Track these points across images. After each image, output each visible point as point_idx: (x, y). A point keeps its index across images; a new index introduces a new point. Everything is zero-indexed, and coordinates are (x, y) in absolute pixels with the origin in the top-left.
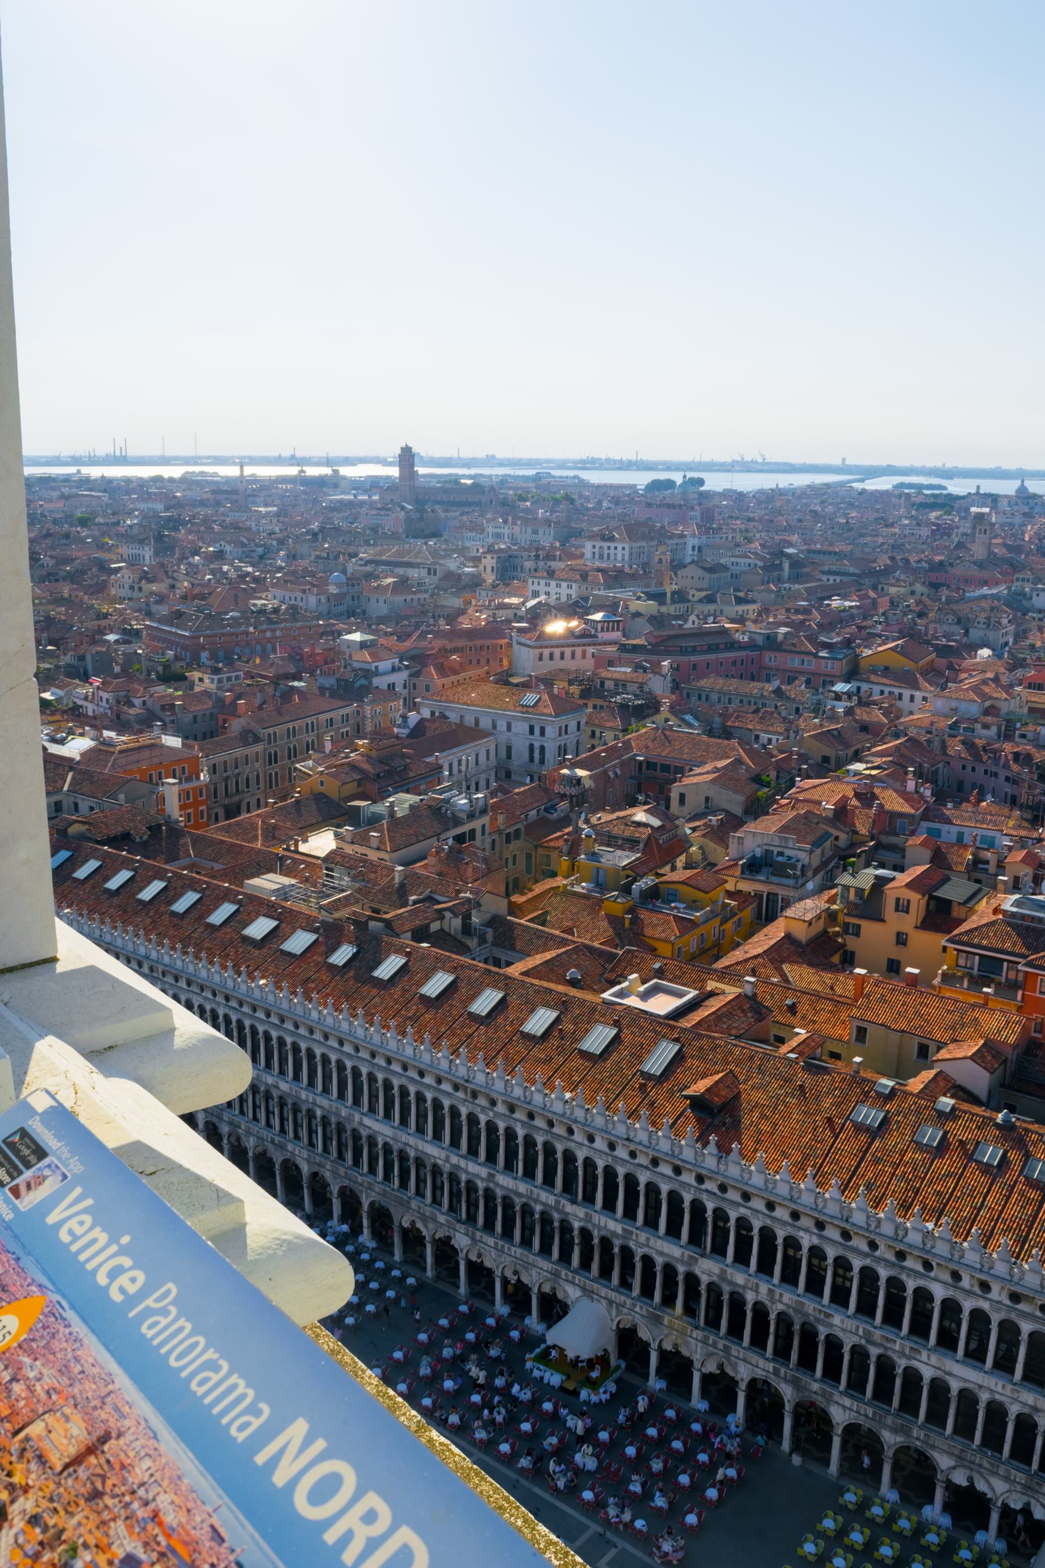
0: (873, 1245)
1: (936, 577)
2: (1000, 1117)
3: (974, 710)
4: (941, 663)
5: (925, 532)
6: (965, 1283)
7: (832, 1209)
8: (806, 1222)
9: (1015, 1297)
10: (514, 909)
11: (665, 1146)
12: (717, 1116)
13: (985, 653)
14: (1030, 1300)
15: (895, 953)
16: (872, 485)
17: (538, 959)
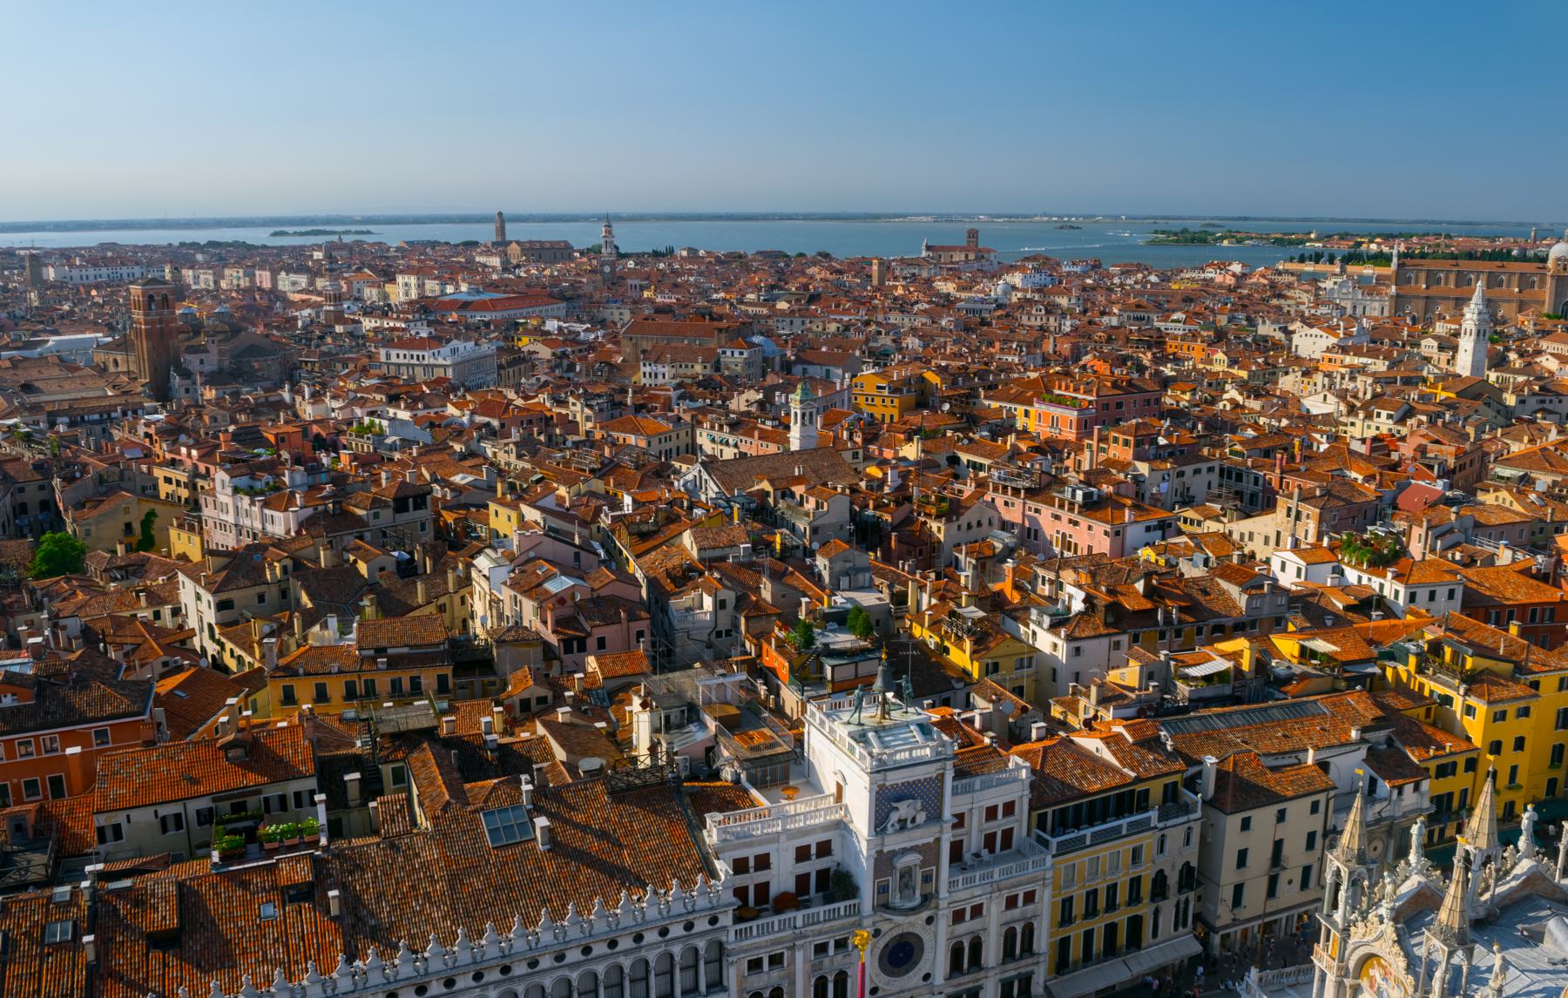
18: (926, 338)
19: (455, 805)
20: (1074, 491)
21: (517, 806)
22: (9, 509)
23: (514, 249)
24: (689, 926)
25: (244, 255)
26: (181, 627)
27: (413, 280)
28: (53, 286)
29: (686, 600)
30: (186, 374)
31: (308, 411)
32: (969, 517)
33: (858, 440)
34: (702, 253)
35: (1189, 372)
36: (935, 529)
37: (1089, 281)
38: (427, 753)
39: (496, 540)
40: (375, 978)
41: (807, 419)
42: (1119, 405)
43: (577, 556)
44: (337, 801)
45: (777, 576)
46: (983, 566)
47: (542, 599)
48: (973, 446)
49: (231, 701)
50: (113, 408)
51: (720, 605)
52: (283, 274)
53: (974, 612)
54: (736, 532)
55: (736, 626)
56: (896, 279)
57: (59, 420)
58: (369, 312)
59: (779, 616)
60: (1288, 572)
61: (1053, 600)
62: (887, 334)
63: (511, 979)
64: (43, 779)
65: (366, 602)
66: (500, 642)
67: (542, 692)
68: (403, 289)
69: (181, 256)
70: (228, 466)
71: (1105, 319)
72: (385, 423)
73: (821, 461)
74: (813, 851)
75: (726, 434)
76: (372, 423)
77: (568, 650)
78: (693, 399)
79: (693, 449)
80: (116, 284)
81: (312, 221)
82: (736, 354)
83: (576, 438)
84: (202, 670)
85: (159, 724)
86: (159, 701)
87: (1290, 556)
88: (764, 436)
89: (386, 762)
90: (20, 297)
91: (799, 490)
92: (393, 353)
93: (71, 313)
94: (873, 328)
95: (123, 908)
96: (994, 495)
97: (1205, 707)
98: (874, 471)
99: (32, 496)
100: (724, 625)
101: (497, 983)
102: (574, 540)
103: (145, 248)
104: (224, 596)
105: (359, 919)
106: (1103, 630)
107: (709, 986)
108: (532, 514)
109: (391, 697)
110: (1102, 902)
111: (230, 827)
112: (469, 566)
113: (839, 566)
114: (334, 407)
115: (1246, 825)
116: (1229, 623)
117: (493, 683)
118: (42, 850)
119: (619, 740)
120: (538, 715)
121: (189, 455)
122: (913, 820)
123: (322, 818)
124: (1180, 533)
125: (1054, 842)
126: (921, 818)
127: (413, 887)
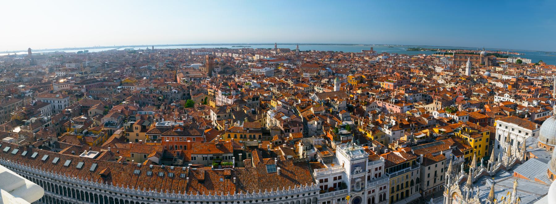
0: (143, 198)
1: (134, 65)
2: (162, 166)
3: (144, 89)
4: (137, 81)
5: (131, 57)
6: (162, 201)
7: (133, 192)
8: (129, 196)
9: (171, 201)
10: (59, 140)
11: (97, 186)
12: (106, 178)
13: (145, 78)
14: (174, 201)
15: (137, 138)
16: (120, 49)
17: (65, 150)
19: (261, 163)
21: (273, 164)
29: (311, 122)
38: (255, 152)
39: (272, 108)
40: (241, 197)
41: (338, 85)
44: (237, 159)
45: (331, 118)
48: (372, 91)
51: (318, 123)
53: (372, 126)
60: (436, 115)
61: (389, 123)
64: (183, 146)
66: (272, 129)
67: (280, 140)
77: (286, 132)
87: (436, 112)
88: (329, 88)
91: (336, 99)
95: (194, 174)
98: (352, 96)
102: (288, 108)
109: (249, 139)
113: (344, 116)
118: (181, 159)
120: (279, 145)
123: (234, 162)
124: (414, 108)
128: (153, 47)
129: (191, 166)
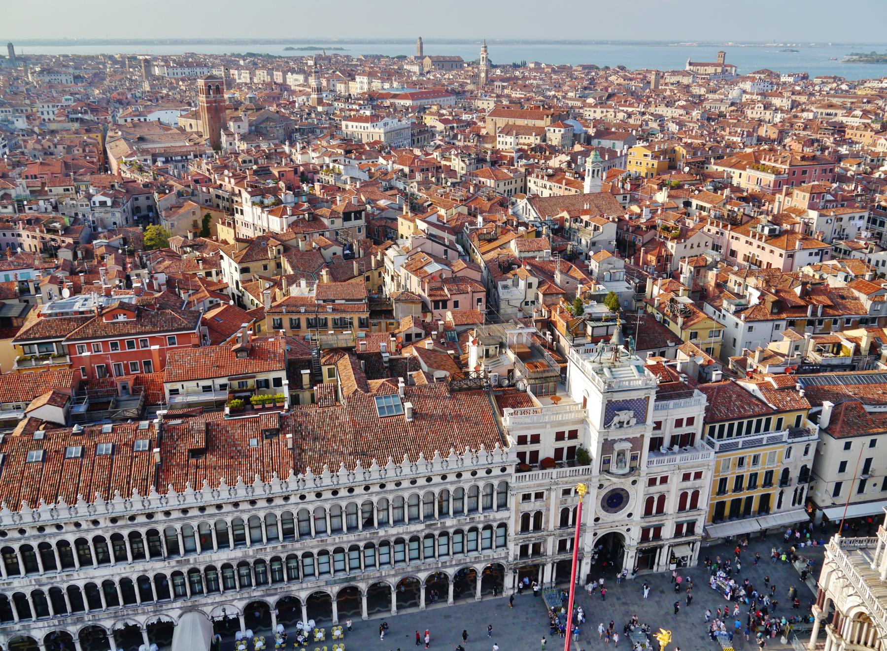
18: (681, 124)
20: (763, 227)
22: (130, 210)
23: (427, 61)
24: (489, 471)
25: (268, 62)
26: (220, 281)
27: (365, 79)
28: (158, 78)
30: (230, 134)
31: (299, 158)
32: (694, 239)
33: (628, 186)
34: (543, 65)
35: (858, 152)
36: (669, 247)
37: (798, 88)
42: (804, 172)
43: (446, 251)
46: (698, 272)
47: (424, 278)
49: (244, 325)
50: (189, 153)
52: (289, 73)
54: (543, 243)
55: (537, 298)
56: (666, 84)
57: (159, 159)
58: (338, 98)
59: (563, 294)
62: (656, 120)
63: (385, 492)
65: (324, 272)
66: (398, 300)
67: (419, 330)
68: (359, 85)
69: (229, 62)
70: (249, 189)
71: (805, 115)
72: (342, 167)
73: (600, 202)
74: (566, 435)
75: (545, 181)
76: (334, 167)
78: (527, 158)
79: (524, 189)
80: (193, 79)
81: (309, 42)
82: (557, 131)
83: (454, 180)
84: (231, 306)
85: (205, 336)
86: (205, 322)
89: (324, 365)
90: (138, 85)
92: (350, 124)
93: (167, 95)
94: (646, 117)
96: (710, 227)
97: (832, 371)
99: (142, 202)
100: (530, 298)
101: (377, 493)
103: (211, 56)
104: (245, 265)
105: (303, 451)
106: (769, 317)
107: (499, 507)
108: (422, 226)
110: (746, 483)
111: (237, 395)
112: (383, 254)
114: (313, 157)
115: (848, 446)
116: (855, 317)
117: (392, 324)
119: (461, 364)
121: (230, 182)
122: (628, 423)
125: (718, 444)
126: (633, 421)
127: (334, 436)
128: (10, 46)
129: (165, 417)
